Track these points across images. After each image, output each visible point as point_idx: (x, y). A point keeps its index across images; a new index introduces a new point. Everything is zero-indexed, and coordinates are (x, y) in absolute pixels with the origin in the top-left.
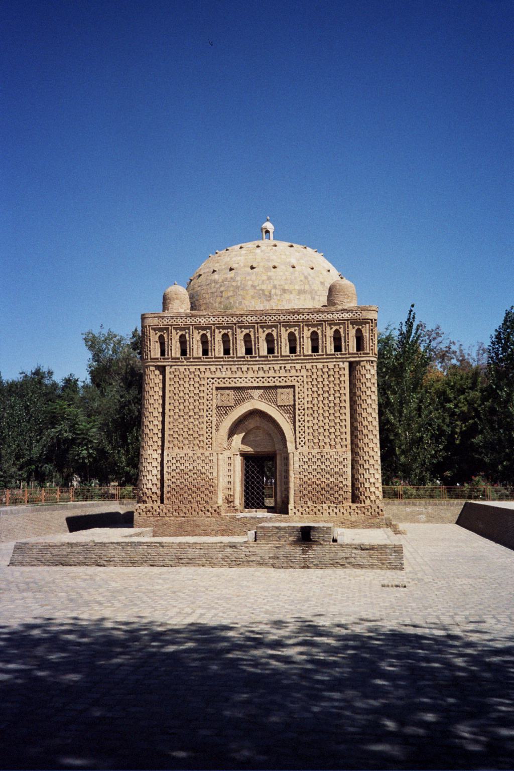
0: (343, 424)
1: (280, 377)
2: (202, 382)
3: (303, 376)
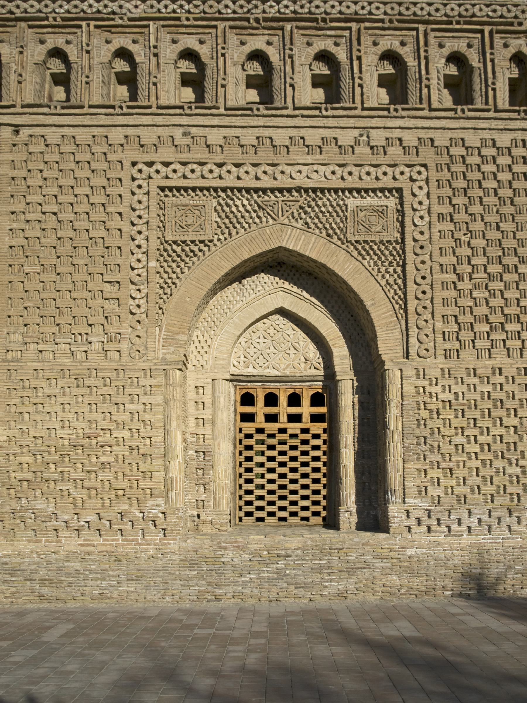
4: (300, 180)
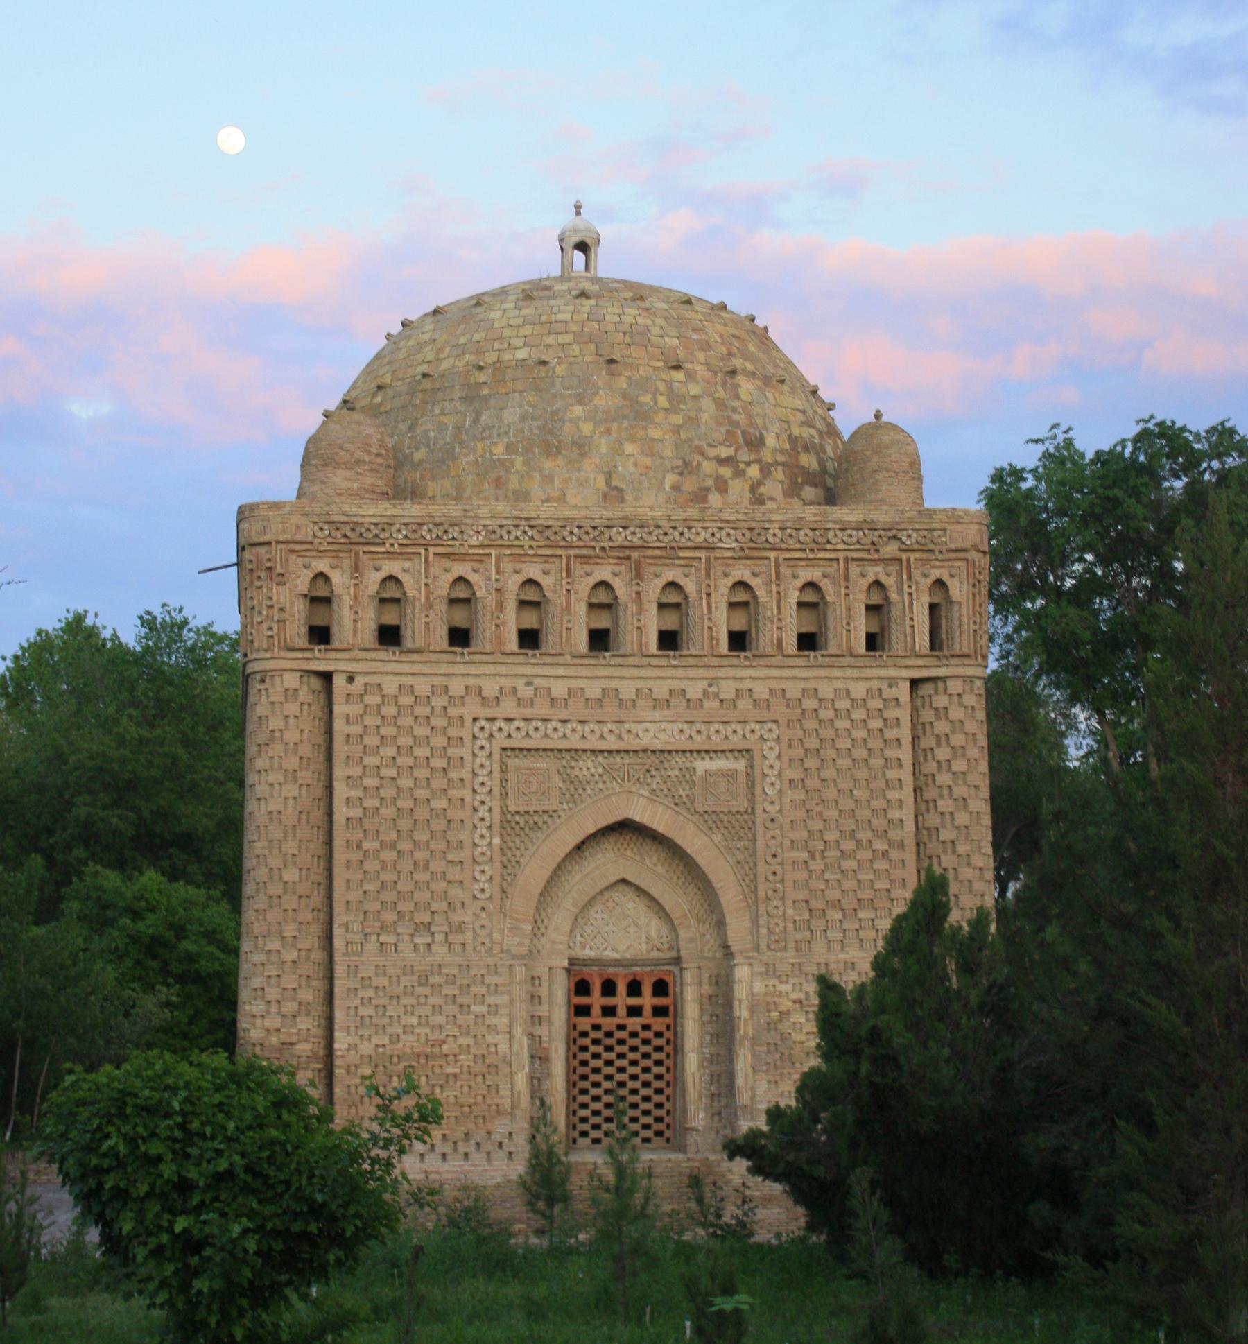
2: (454, 732)
4: (646, 741)
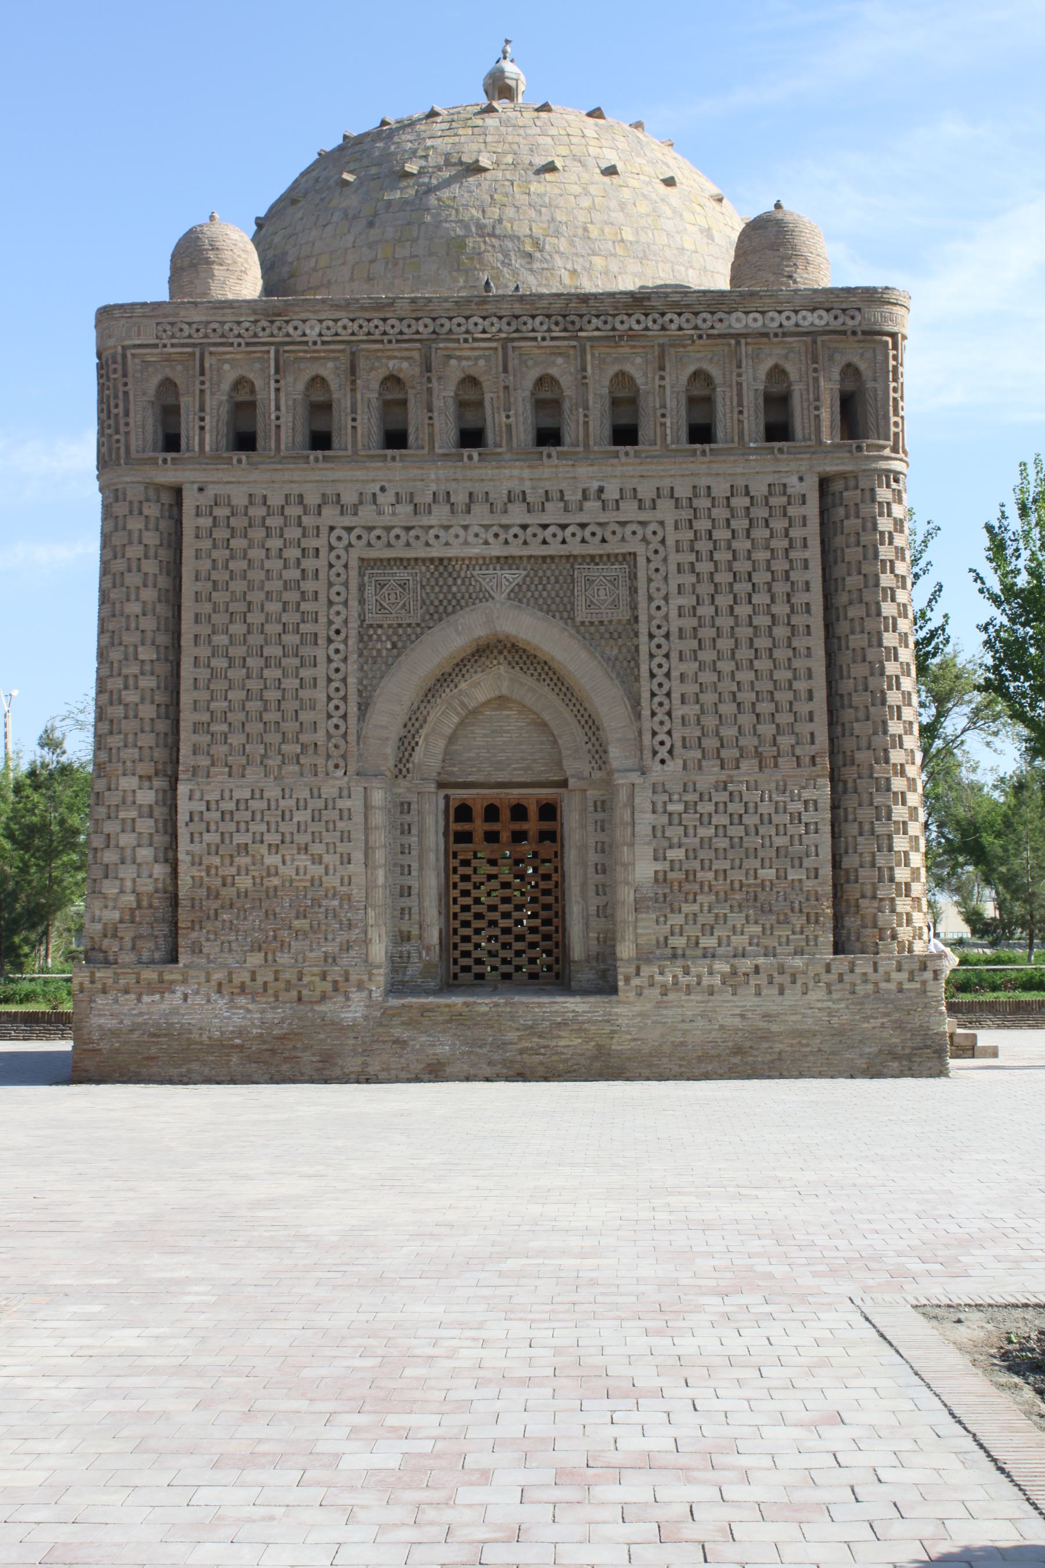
0: (801, 686)
1: (583, 526)
2: (311, 543)
3: (662, 523)
